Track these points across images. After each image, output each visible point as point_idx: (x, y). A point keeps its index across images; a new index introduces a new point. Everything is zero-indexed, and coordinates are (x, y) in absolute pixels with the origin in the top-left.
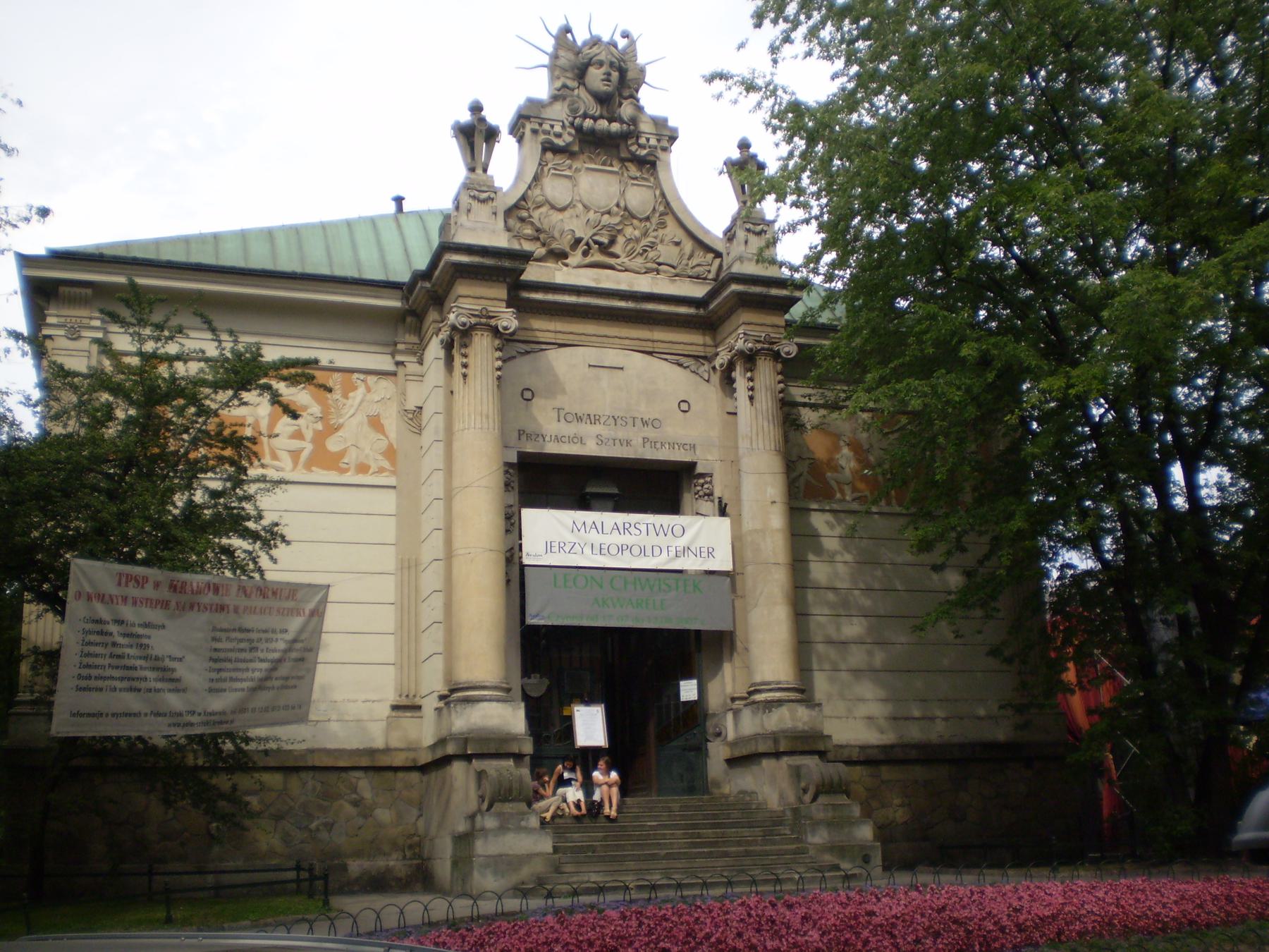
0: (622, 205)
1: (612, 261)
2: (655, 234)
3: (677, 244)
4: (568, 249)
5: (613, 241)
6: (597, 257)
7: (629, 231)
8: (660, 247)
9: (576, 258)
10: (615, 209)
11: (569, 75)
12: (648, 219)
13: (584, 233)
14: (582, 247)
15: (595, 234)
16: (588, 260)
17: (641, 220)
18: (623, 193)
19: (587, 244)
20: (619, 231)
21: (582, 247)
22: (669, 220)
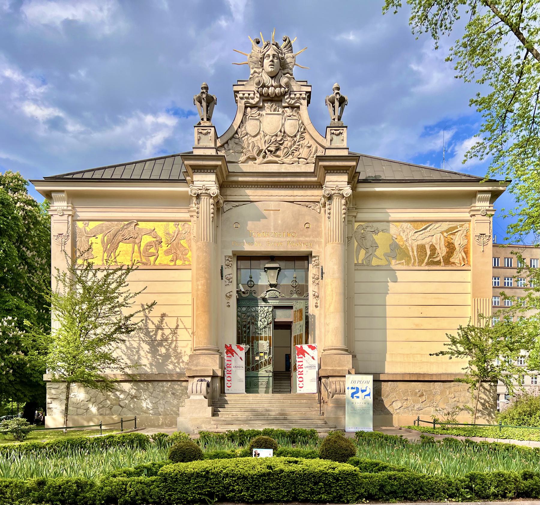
0: (283, 131)
3: (309, 147)
4: (256, 156)
5: (278, 149)
6: (270, 158)
8: (301, 150)
9: (260, 159)
10: (279, 133)
11: (256, 66)
12: (295, 136)
14: (262, 154)
15: (268, 147)
16: (266, 160)
17: (292, 137)
18: (283, 125)
19: (265, 152)
20: (281, 144)
21: (262, 154)
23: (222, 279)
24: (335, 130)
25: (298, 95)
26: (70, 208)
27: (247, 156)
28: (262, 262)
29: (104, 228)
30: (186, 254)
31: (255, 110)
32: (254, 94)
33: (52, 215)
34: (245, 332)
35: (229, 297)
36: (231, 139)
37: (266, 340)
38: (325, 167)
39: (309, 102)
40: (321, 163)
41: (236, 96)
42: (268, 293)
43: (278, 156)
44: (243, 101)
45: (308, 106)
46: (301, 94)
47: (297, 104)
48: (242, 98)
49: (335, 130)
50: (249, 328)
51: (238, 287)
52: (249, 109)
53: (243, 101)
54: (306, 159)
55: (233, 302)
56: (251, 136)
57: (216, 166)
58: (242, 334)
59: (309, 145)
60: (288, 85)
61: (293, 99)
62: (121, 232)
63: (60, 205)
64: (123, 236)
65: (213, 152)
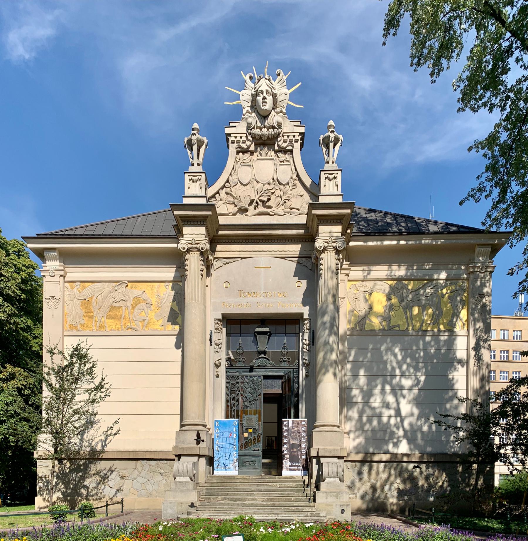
0: (275, 179)
1: (269, 210)
2: (291, 192)
4: (247, 207)
5: (269, 200)
6: (261, 209)
7: (278, 193)
10: (272, 181)
13: (256, 198)
14: (254, 204)
16: (258, 211)
17: (284, 185)
19: (257, 202)
20: (273, 193)
21: (254, 204)
22: (297, 182)
23: (211, 345)
24: (329, 174)
25: (291, 137)
26: (62, 268)
27: (238, 207)
28: (252, 326)
29: (96, 290)
30: (177, 318)
31: (247, 155)
32: (247, 137)
33: (44, 276)
34: (234, 405)
35: (217, 366)
36: (222, 188)
37: (255, 414)
38: (318, 216)
39: (302, 146)
40: (314, 212)
41: (228, 140)
42: (258, 361)
43: (270, 207)
44: (235, 145)
45: (301, 150)
46: (294, 136)
47: (290, 148)
48: (233, 142)
49: (329, 174)
50: (238, 400)
51: (228, 354)
52: (241, 154)
53: (235, 145)
54: (298, 210)
55: (222, 370)
56: (241, 184)
57: (205, 217)
58: (231, 408)
59: (301, 194)
60: (279, 125)
61: (285, 141)
62: (112, 294)
63: (53, 264)
64: (113, 298)
65: (203, 201)
